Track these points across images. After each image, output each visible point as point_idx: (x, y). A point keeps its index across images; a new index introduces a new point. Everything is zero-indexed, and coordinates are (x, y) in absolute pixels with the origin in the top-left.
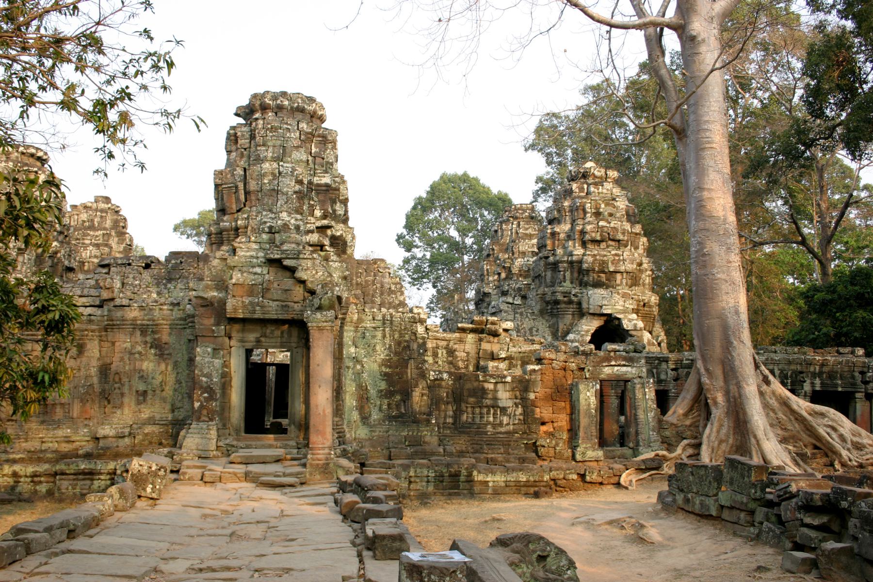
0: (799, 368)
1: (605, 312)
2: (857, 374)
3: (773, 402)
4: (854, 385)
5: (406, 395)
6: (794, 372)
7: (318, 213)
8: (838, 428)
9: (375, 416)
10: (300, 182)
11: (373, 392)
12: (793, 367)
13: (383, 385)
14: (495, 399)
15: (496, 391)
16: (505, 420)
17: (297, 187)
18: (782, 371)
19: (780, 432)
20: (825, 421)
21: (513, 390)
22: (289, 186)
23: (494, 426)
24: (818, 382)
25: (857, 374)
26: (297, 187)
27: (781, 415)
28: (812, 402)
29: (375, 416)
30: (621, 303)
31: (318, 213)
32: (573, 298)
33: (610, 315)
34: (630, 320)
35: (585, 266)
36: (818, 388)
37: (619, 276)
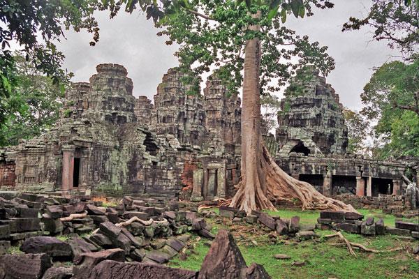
0: (325, 164)
1: (297, 138)
2: (356, 167)
3: (279, 180)
4: (354, 173)
5: (135, 175)
6: (322, 166)
7: (113, 108)
8: (310, 193)
9: (125, 181)
10: (104, 97)
11: (125, 174)
12: (321, 164)
13: (128, 171)
14: (167, 176)
15: (167, 173)
16: (170, 184)
17: (103, 100)
18: (316, 166)
19: (282, 192)
20: (303, 188)
21: (173, 173)
22: (100, 99)
23: (166, 186)
24: (334, 171)
25: (356, 167)
26: (103, 100)
27: (282, 185)
28: (300, 180)
29: (125, 181)
30: (306, 134)
31: (113, 108)
32: (285, 133)
33: (299, 140)
34: (308, 142)
35: (290, 117)
36: (334, 174)
37: (307, 122)
